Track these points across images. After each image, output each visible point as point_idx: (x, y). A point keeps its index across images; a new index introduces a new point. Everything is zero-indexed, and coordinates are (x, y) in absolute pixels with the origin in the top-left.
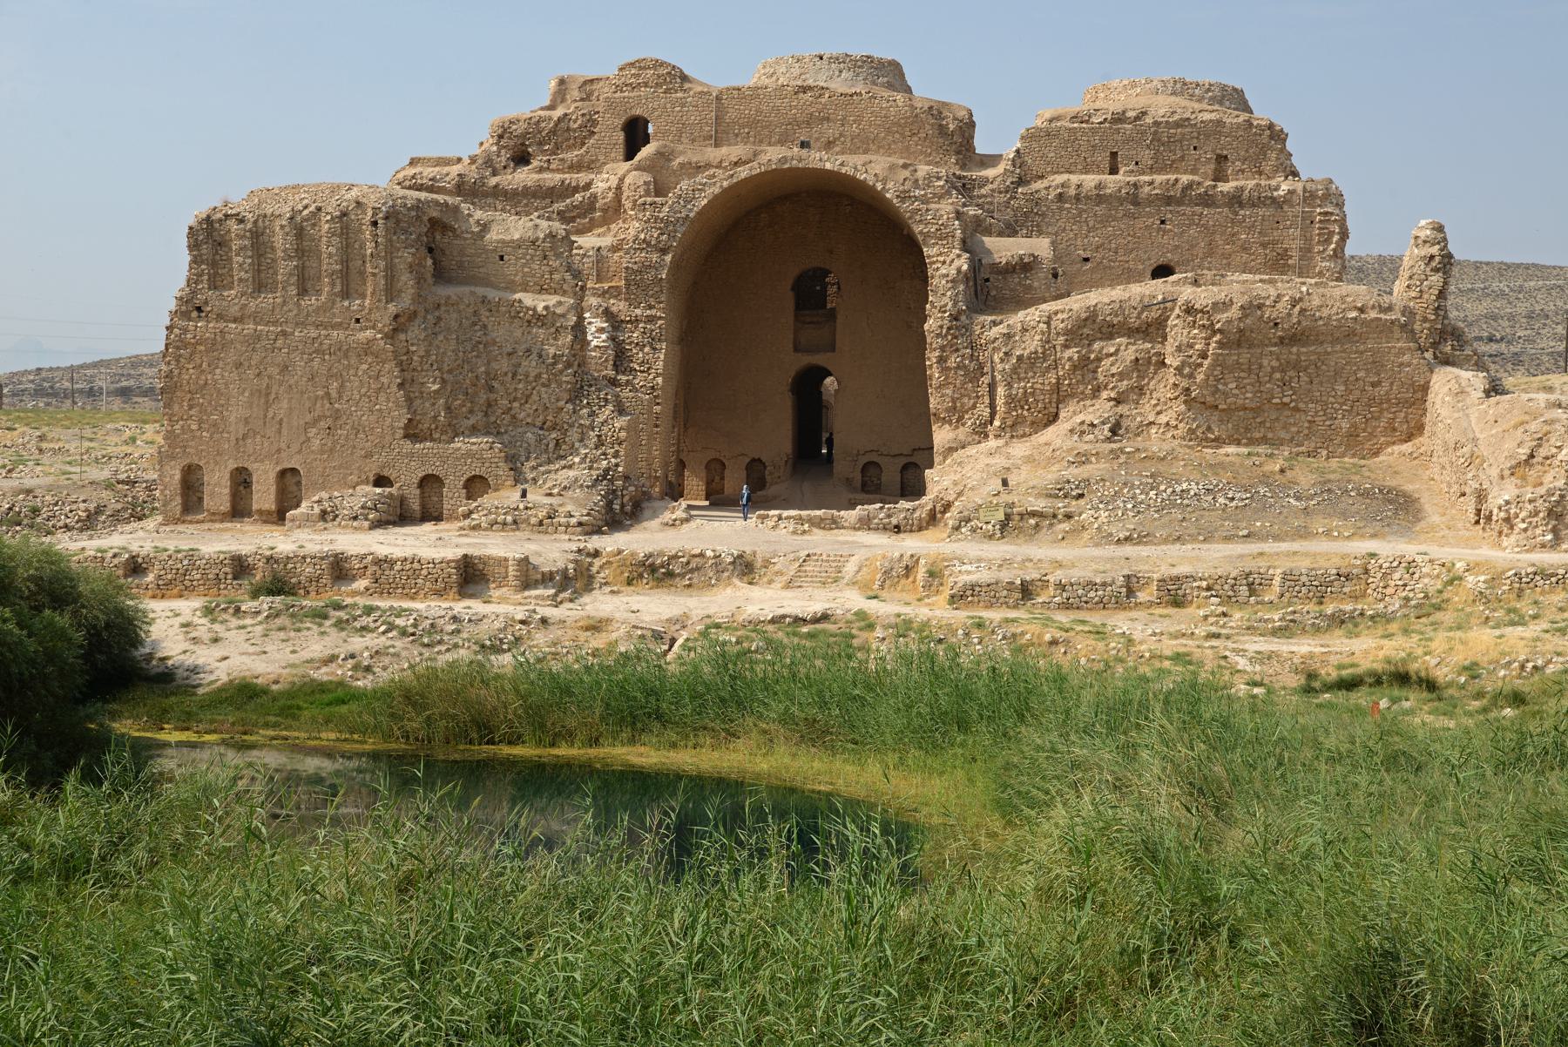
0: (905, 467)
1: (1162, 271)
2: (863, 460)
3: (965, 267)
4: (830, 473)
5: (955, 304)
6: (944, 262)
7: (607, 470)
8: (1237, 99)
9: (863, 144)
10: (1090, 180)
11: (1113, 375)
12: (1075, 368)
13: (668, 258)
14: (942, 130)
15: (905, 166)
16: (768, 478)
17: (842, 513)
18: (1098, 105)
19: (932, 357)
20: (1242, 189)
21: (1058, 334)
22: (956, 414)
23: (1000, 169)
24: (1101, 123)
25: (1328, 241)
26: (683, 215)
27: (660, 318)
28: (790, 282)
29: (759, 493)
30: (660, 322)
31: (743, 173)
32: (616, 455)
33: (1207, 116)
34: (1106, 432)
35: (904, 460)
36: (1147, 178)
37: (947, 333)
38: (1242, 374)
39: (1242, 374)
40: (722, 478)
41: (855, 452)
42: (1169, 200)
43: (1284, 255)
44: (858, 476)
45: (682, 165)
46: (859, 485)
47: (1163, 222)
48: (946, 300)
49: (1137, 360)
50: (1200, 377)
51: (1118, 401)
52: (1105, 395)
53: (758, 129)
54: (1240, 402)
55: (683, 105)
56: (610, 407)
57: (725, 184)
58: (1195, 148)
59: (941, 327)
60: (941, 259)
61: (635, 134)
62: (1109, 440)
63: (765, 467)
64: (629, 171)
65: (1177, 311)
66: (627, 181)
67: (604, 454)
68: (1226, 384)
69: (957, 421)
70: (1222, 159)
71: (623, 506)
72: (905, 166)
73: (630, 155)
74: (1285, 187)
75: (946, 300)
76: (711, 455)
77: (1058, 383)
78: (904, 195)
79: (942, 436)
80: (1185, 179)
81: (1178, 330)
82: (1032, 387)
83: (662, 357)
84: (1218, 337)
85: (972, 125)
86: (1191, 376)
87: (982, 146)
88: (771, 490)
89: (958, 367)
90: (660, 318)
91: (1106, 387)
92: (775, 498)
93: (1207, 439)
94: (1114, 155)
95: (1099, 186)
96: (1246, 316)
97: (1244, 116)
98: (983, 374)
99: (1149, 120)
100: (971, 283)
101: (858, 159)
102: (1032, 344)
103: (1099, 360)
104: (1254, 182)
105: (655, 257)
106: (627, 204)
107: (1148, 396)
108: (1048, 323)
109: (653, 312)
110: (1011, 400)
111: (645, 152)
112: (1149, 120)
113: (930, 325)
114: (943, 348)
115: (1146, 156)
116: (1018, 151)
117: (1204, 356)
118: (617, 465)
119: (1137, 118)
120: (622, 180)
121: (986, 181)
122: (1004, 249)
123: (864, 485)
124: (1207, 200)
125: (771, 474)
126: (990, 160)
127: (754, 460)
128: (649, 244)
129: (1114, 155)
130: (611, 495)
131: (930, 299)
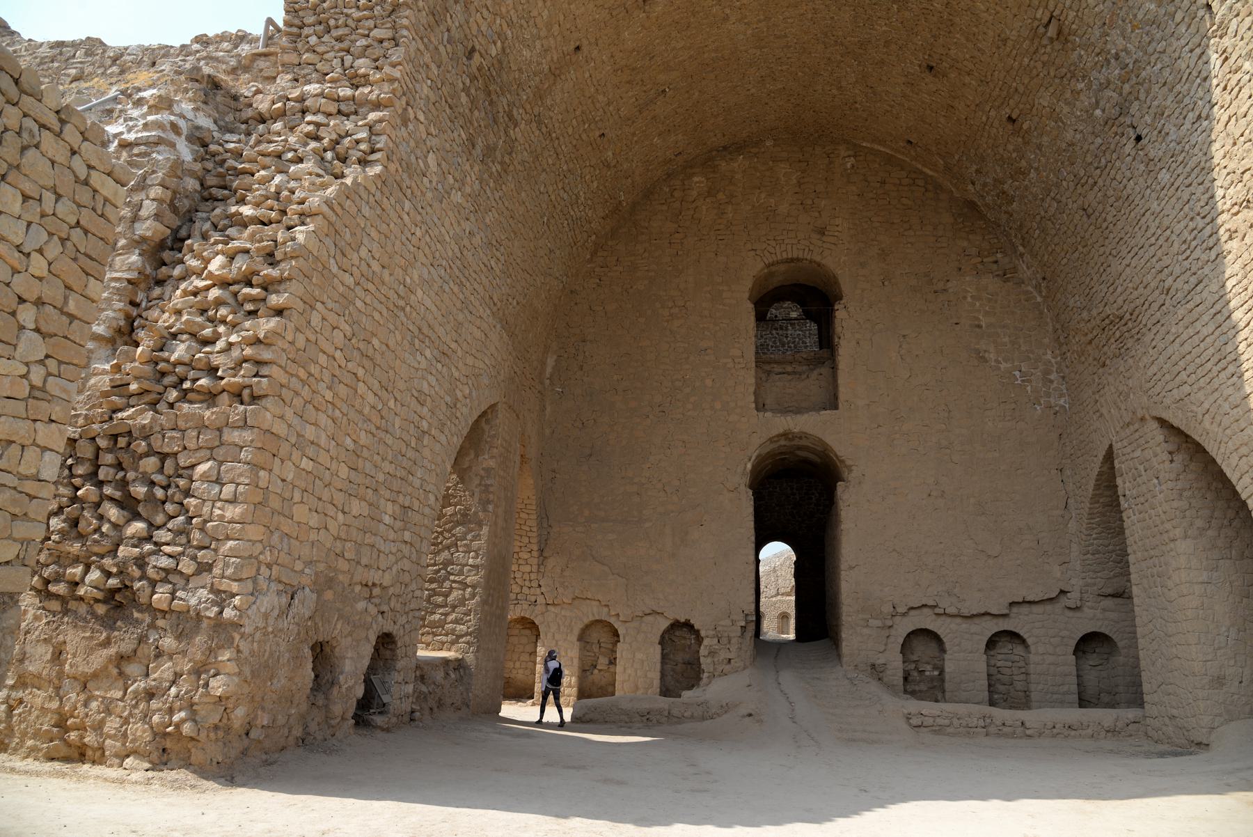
0: (992, 643)
2: (904, 627)
16: (705, 662)
28: (748, 284)
29: (687, 694)
30: (373, 116)
35: (993, 627)
40: (613, 662)
41: (887, 609)
44: (895, 663)
63: (699, 640)
76: (593, 612)
88: (713, 691)
90: (377, 106)
92: (726, 708)
125: (712, 653)
127: (676, 625)
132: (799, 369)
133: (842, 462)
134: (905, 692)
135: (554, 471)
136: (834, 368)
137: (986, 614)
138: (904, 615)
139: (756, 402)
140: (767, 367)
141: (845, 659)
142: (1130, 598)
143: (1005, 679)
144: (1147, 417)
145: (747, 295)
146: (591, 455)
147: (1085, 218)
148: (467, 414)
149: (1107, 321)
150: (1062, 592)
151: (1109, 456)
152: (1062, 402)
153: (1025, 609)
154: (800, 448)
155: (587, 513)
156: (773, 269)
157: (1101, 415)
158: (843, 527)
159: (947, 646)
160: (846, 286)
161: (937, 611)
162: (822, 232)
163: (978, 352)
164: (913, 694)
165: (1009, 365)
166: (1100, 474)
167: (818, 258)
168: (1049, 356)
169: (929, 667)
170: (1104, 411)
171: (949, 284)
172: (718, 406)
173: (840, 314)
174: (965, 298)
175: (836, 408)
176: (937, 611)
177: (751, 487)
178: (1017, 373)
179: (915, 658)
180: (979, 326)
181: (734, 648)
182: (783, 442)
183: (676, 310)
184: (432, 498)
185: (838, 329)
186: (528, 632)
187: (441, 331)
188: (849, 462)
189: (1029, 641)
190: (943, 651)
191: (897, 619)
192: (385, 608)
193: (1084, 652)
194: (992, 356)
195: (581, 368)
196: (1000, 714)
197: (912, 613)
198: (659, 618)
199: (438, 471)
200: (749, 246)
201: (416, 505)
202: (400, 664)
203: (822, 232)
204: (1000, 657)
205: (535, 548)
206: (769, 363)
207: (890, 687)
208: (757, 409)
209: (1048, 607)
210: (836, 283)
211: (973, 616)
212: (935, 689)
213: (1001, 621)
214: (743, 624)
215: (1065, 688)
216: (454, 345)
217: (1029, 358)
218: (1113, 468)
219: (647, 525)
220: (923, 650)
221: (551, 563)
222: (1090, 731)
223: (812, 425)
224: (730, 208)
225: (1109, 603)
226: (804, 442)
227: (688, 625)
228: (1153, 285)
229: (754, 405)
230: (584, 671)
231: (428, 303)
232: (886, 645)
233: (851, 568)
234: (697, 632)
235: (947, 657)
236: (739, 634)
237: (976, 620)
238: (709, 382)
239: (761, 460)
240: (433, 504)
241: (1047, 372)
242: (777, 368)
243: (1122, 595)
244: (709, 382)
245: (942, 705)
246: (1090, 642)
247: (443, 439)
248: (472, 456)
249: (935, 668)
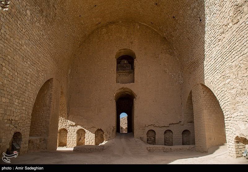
0: (165, 132)
2: (147, 129)
35: (166, 129)
46: (146, 140)
127: (99, 130)
132: (126, 74)
133: (135, 94)
134: (147, 143)
135: (71, 96)
136: (134, 74)
138: (148, 127)
139: (116, 81)
140: (119, 74)
141: (135, 136)
142: (194, 123)
143: (168, 140)
144: (199, 84)
145: (115, 57)
146: (79, 92)
147: (188, 40)
148: (42, 80)
149: (192, 63)
150: (180, 122)
151: (191, 93)
152: (182, 82)
153: (172, 125)
154: (126, 91)
155: (78, 105)
156: (121, 51)
157: (190, 84)
158: (135, 108)
159: (156, 133)
160: (137, 56)
161: (154, 126)
162: (132, 43)
163: (165, 71)
164: (149, 143)
165: (171, 74)
166: (189, 97)
167: (131, 49)
168: (179, 72)
169: (152, 138)
170: (190, 83)
171: (159, 56)
172: (108, 81)
173: (135, 62)
174: (162, 59)
176: (154, 126)
178: (172, 75)
179: (150, 136)
180: (165, 65)
181: (111, 135)
182: (122, 90)
184: (32, 100)
185: (135, 65)
186: (65, 132)
187: (33, 58)
188: (136, 94)
189: (173, 132)
190: (156, 134)
191: (146, 128)
192: (17, 126)
193: (184, 134)
194: (168, 72)
196: (166, 147)
197: (149, 126)
198: (95, 128)
199: (34, 93)
200: (115, 46)
201: (27, 101)
202: (23, 140)
203: (132, 43)
204: (167, 135)
205: (66, 113)
206: (120, 73)
207: (144, 142)
208: (117, 82)
209: (177, 125)
210: (135, 55)
211: (162, 127)
212: (154, 142)
213: (167, 128)
214: (113, 129)
215: (180, 141)
216: (38, 62)
217: (175, 72)
218: (191, 95)
219: (92, 108)
220: (151, 134)
221: (70, 116)
222: (184, 150)
223: (128, 86)
225: (189, 124)
226: (127, 90)
227: (101, 130)
228: (202, 54)
229: (116, 82)
230: (78, 140)
231: (28, 50)
232: (143, 133)
235: (156, 135)
236: (112, 131)
237: (162, 128)
238: (106, 76)
239: (117, 94)
240: (33, 101)
241: (179, 75)
242: (122, 74)
243: (192, 122)
244: (106, 76)
245: (155, 146)
246: (185, 132)
247: (35, 85)
248: (47, 91)
249: (154, 138)
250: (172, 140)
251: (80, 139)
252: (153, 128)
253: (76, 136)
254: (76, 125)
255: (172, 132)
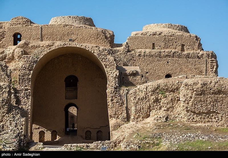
0: (98, 132)
1: (168, 76)
2: (85, 131)
3: (118, 74)
4: (76, 134)
5: (115, 85)
6: (112, 73)
7: (19, 133)
8: (185, 29)
9: (83, 40)
10: (148, 51)
11: (165, 103)
12: (154, 102)
13: (32, 72)
14: (106, 37)
15: (96, 47)
17: (89, 144)
18: (148, 30)
19: (109, 99)
20: (189, 54)
21: (149, 92)
22: (116, 115)
23: (122, 48)
24: (150, 35)
25: (213, 68)
26: (36, 60)
27: (29, 89)
30: (29, 91)
31: (53, 48)
32: (22, 129)
33: (179, 34)
34: (164, 120)
35: (97, 130)
36: (163, 50)
37: (113, 92)
38: (202, 103)
39: (202, 103)
41: (83, 128)
42: (169, 56)
43: (201, 72)
45: (32, 46)
46: (85, 137)
47: (168, 62)
48: (113, 83)
49: (172, 99)
50: (190, 104)
51: (168, 110)
52: (163, 109)
53: (53, 36)
54: (202, 111)
55: (31, 30)
56: (19, 115)
57: (48, 51)
58: (176, 42)
59: (112, 91)
60: (110, 72)
61: (16, 38)
62: (166, 121)
64: (16, 48)
65: (183, 85)
66: (16, 50)
67: (18, 129)
68: (197, 106)
69: (117, 118)
70: (183, 46)
71: (24, 144)
72: (96, 47)
73: (15, 44)
74: (201, 53)
75: (113, 83)
77: (150, 106)
78: (99, 55)
79: (112, 122)
80: (173, 51)
81: (183, 91)
82: (142, 107)
83: (30, 100)
84: (195, 92)
85: (113, 36)
86: (188, 103)
87: (116, 42)
89: (117, 102)
90: (29, 89)
91: (163, 107)
93: (193, 122)
94: (154, 44)
95: (150, 53)
96: (202, 87)
97: (188, 34)
98: (124, 104)
99: (163, 34)
100: (120, 79)
101: (84, 45)
102: (142, 95)
103: (161, 99)
104: (192, 52)
105: (28, 72)
106: (16, 58)
107: (175, 109)
108: (147, 89)
109: (27, 87)
110: (136, 111)
111: (20, 43)
112: (163, 34)
113: (108, 90)
114: (112, 97)
115: (163, 44)
116: (127, 43)
117: (191, 98)
118: (22, 132)
119: (160, 34)
120: (14, 50)
121: (118, 51)
122: (129, 69)
123: (86, 137)
124: (179, 56)
126: (120, 45)
127: (53, 131)
128: (26, 68)
129: (154, 44)
130: (20, 141)
131: (108, 83)
137: (97, 128)
153: (102, 127)
162: (76, 71)
167: (75, 75)
175: (77, 99)
177: (64, 110)
183: (53, 83)
190: (91, 133)
191: (85, 129)
194: (100, 91)
195: (38, 92)
203: (76, 71)
207: (83, 138)
211: (95, 129)
224: (61, 66)
233: (78, 122)
234: (56, 132)
238: (58, 95)
244: (58, 95)
250: (102, 137)
251: (41, 137)
252: (89, 129)
253: (38, 135)
254: (39, 128)
255: (102, 132)
